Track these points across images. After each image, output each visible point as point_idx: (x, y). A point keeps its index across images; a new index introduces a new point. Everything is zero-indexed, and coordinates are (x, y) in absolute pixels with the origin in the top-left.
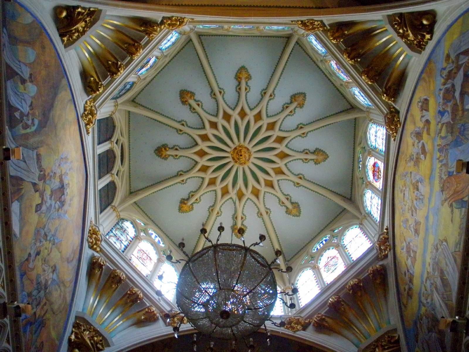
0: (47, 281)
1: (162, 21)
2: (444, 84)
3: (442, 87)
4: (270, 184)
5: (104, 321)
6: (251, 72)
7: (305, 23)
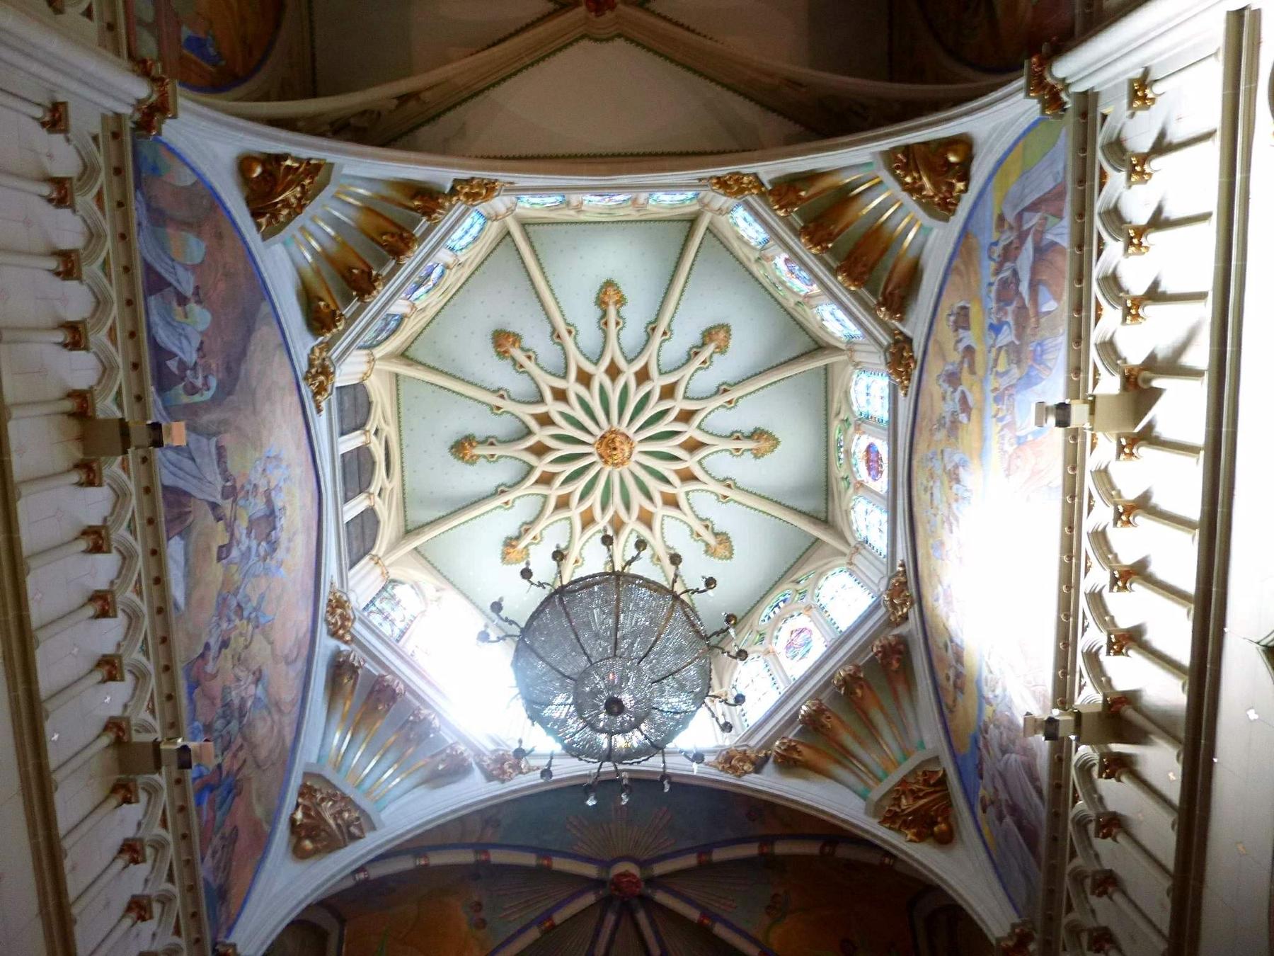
0: (243, 700)
1: (453, 188)
2: (997, 272)
3: (992, 279)
4: (672, 502)
5: (363, 780)
6: (624, 289)
7: (725, 182)
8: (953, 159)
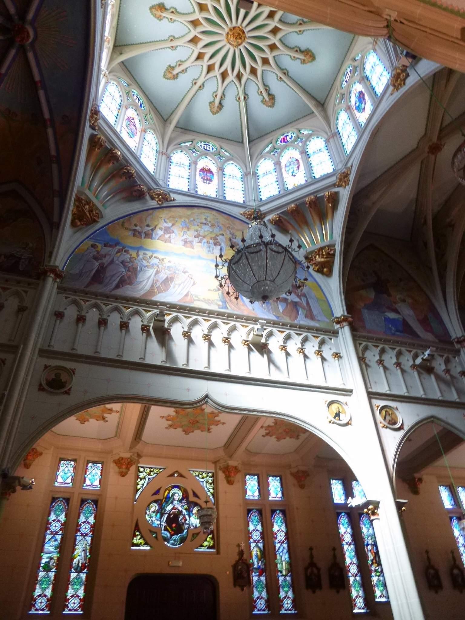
7: (347, 177)
8: (325, 270)
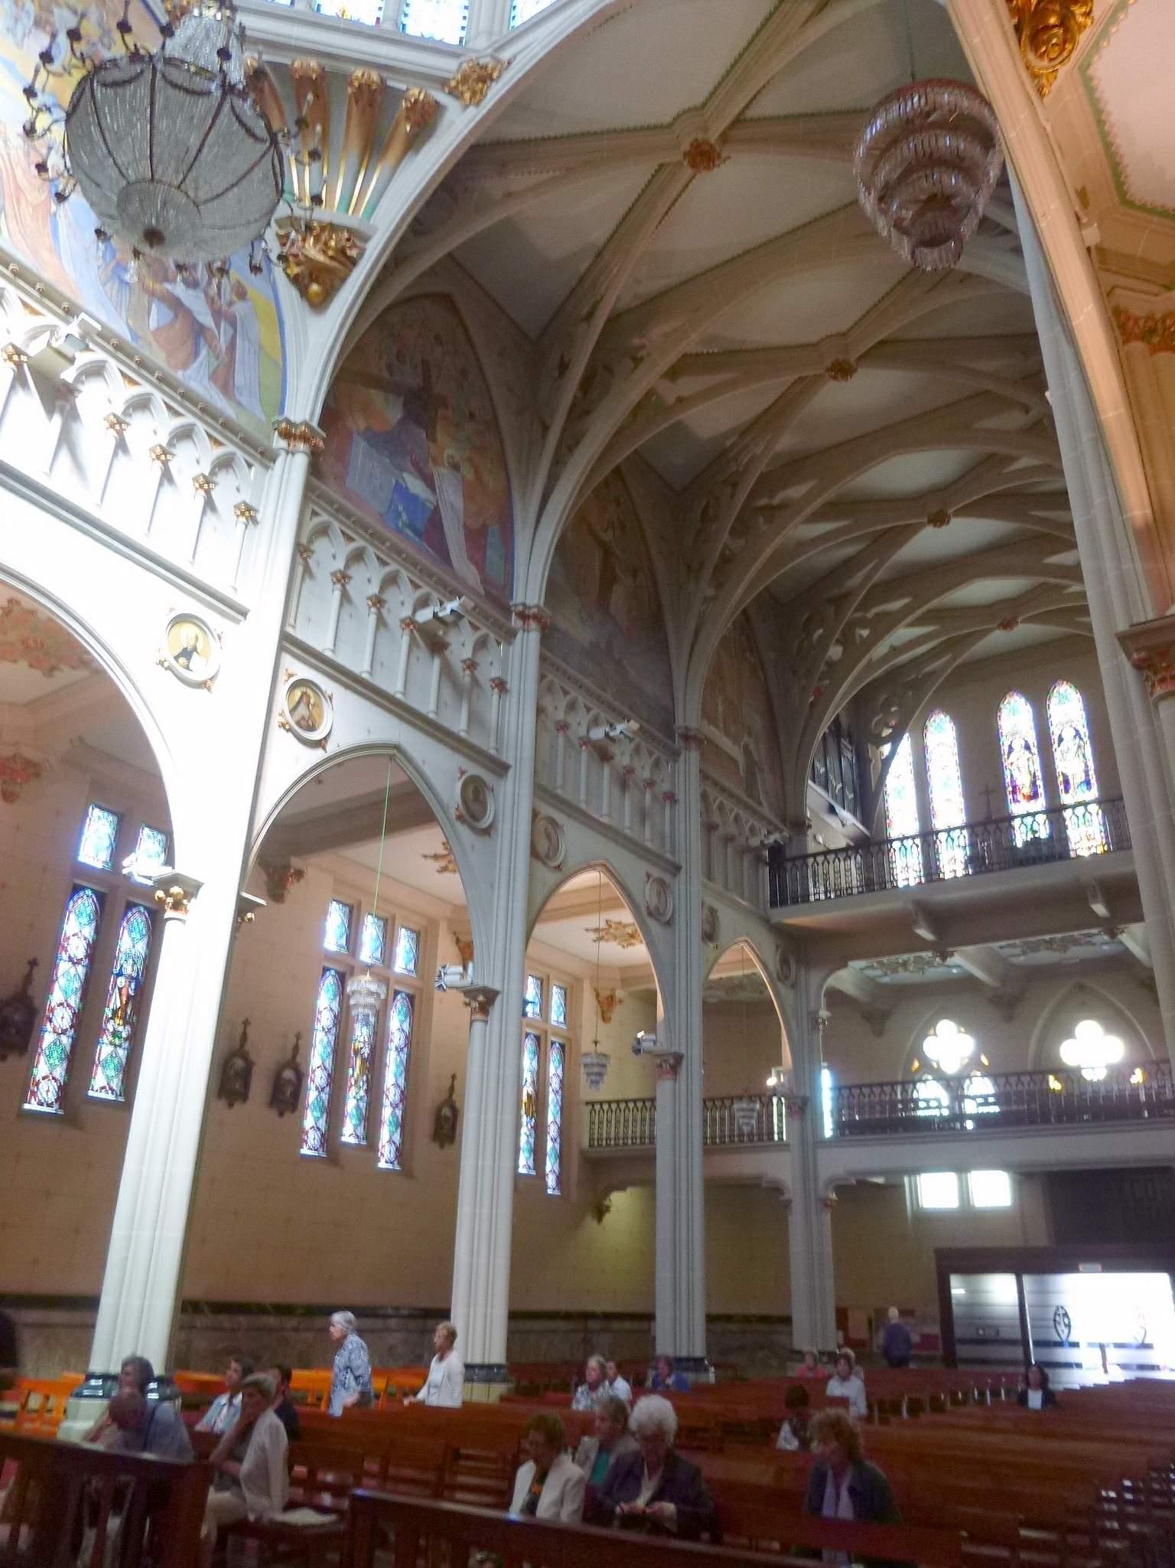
7: (484, 82)
8: (315, 287)
